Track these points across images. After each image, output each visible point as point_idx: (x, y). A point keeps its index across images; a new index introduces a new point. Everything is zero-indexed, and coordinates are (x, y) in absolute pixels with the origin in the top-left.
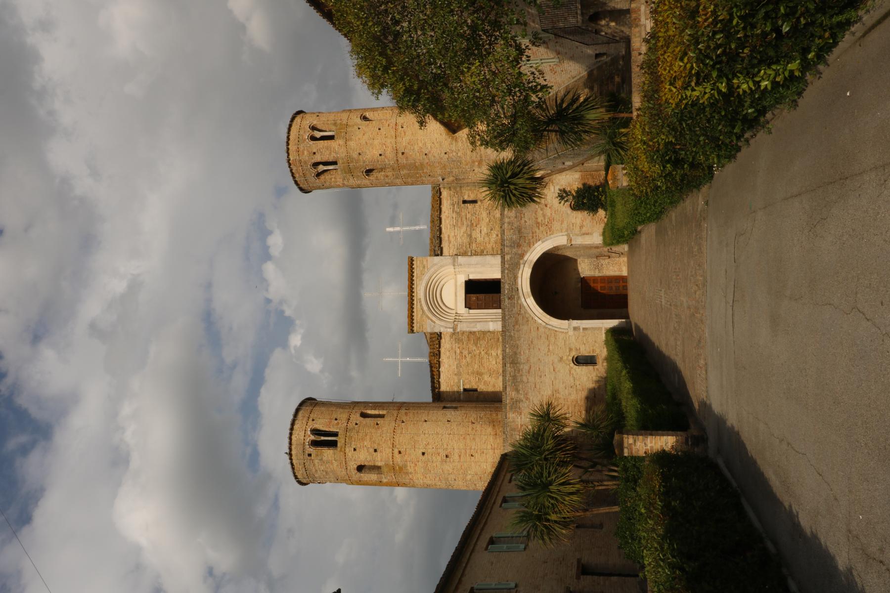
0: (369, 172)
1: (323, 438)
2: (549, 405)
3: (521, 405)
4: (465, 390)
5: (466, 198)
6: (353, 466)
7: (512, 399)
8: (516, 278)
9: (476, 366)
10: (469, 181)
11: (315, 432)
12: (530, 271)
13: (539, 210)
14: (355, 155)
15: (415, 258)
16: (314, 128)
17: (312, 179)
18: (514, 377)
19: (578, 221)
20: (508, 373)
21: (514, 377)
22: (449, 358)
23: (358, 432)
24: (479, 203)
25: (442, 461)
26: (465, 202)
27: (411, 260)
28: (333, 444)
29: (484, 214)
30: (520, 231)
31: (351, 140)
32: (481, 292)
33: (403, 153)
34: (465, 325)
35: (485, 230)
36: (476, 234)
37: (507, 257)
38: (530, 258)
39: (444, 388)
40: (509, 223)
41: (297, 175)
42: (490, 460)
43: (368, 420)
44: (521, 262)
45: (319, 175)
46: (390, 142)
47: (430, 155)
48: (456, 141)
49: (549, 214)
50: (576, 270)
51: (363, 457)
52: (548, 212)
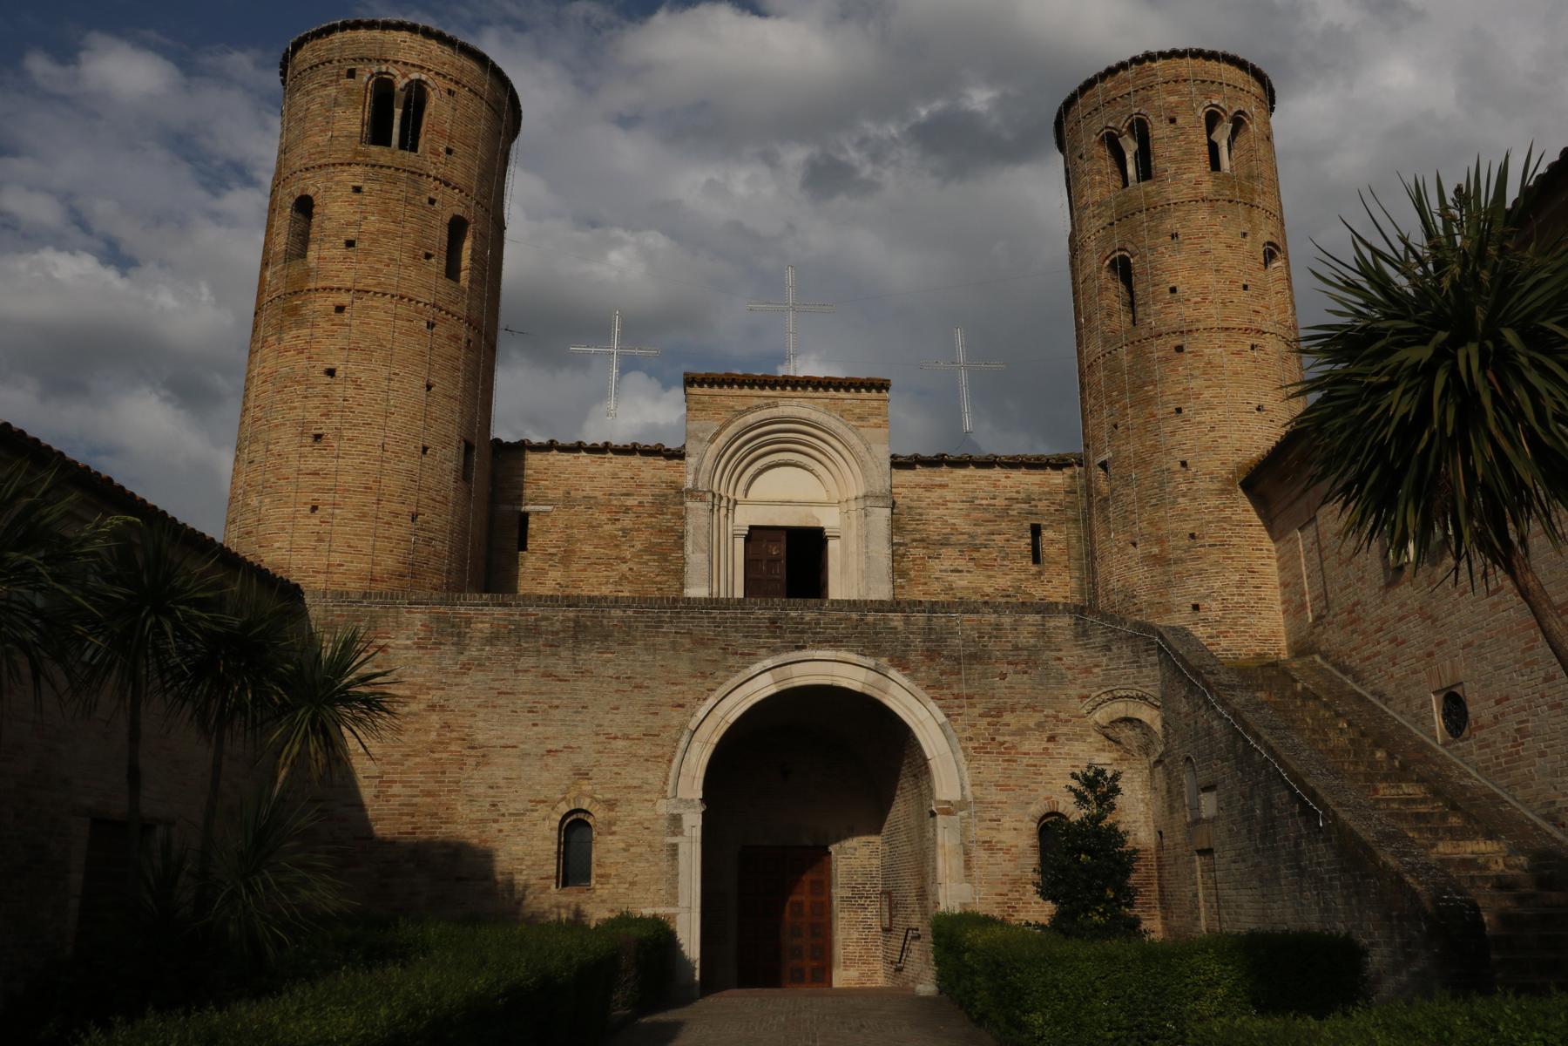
0: (1123, 269)
1: (398, 112)
2: (374, 704)
3: (448, 649)
4: (524, 517)
5: (1047, 534)
6: (313, 185)
7: (469, 622)
8: (835, 642)
9: (588, 549)
10: (1099, 536)
11: (417, 93)
12: (856, 686)
13: (1038, 717)
14: (1171, 224)
15: (884, 394)
16: (1238, 122)
17: (1099, 124)
18: (534, 631)
19: (1006, 837)
20: (548, 613)
21: (534, 631)
22: (614, 476)
23: (408, 201)
24: (1034, 569)
25: (304, 425)
26: (1036, 531)
27: (882, 386)
28: (378, 132)
29: (1003, 582)
30: (974, 658)
31: (1214, 212)
32: (792, 561)
33: (1179, 349)
34: (704, 521)
35: (961, 582)
36: (949, 558)
37: (896, 620)
38: (894, 689)
39: (532, 459)
40: (998, 627)
41: (1109, 84)
42: (296, 560)
43: (440, 236)
44: (884, 661)
45: (1112, 142)
46: (1212, 313)
47: (1177, 421)
48: (1222, 491)
49: (1026, 747)
50: (852, 832)
51: (335, 210)
52: (1034, 744)
